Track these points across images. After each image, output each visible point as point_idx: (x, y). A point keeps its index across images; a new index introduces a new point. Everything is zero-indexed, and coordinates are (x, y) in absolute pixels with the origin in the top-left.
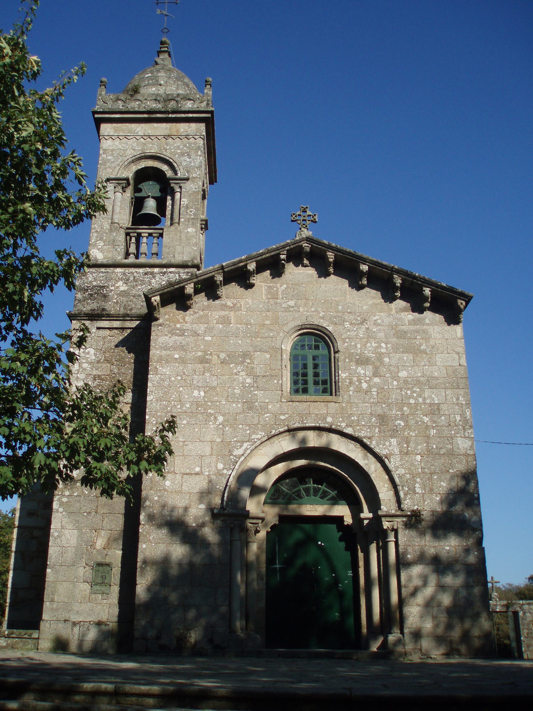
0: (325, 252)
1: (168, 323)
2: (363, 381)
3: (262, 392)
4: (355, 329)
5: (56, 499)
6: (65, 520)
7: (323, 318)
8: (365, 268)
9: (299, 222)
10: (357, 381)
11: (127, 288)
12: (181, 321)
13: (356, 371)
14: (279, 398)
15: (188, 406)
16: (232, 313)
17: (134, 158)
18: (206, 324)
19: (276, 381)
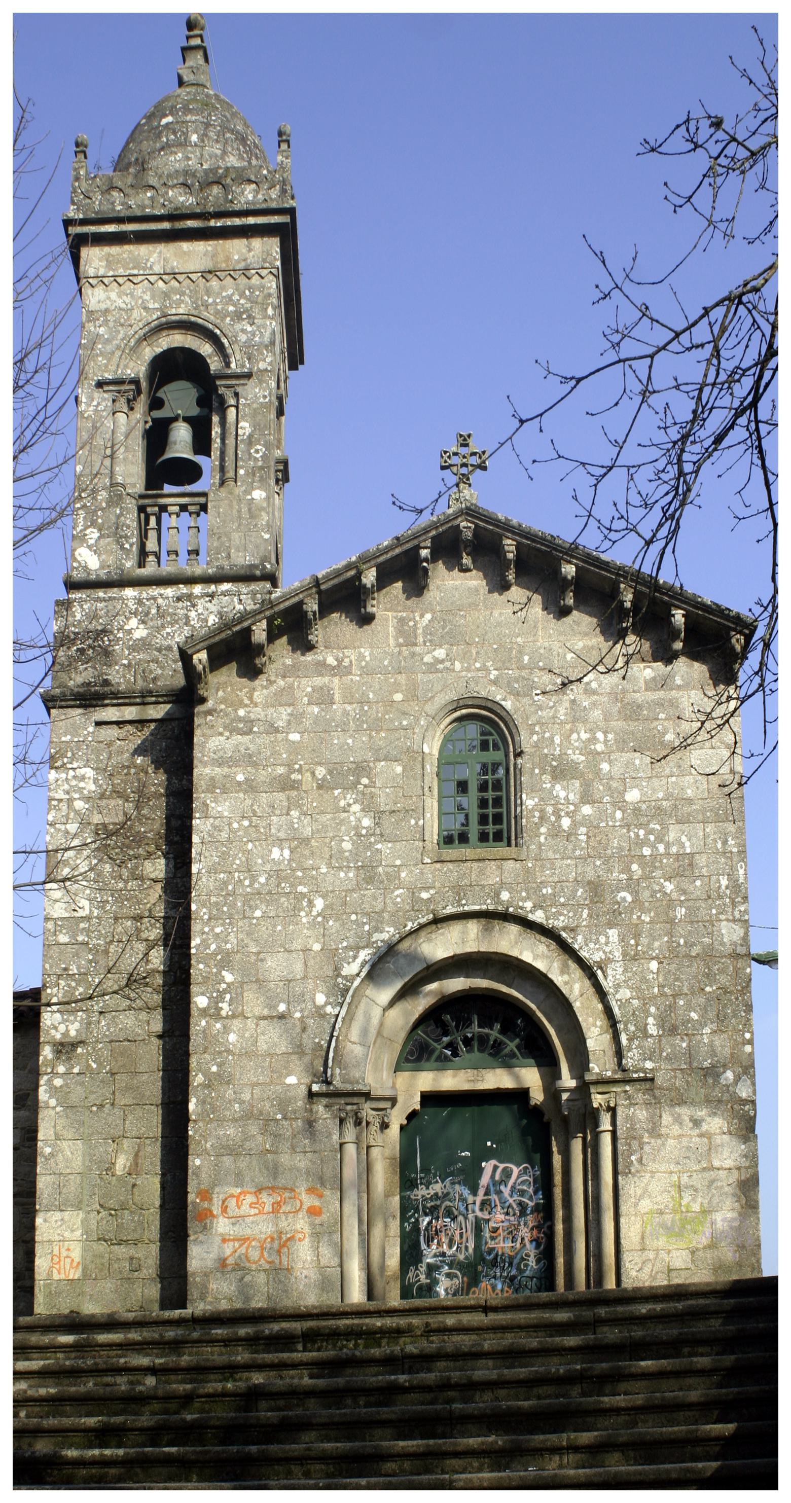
0: (500, 537)
1: (223, 707)
2: (563, 814)
3: (390, 845)
4: (551, 704)
5: (43, 1081)
6: (61, 1122)
7: (495, 682)
8: (569, 570)
9: (455, 469)
10: (554, 813)
11: (146, 632)
12: (246, 701)
13: (551, 793)
14: (419, 856)
15: (262, 880)
16: (336, 680)
17: (147, 329)
18: (289, 705)
19: (413, 822)
